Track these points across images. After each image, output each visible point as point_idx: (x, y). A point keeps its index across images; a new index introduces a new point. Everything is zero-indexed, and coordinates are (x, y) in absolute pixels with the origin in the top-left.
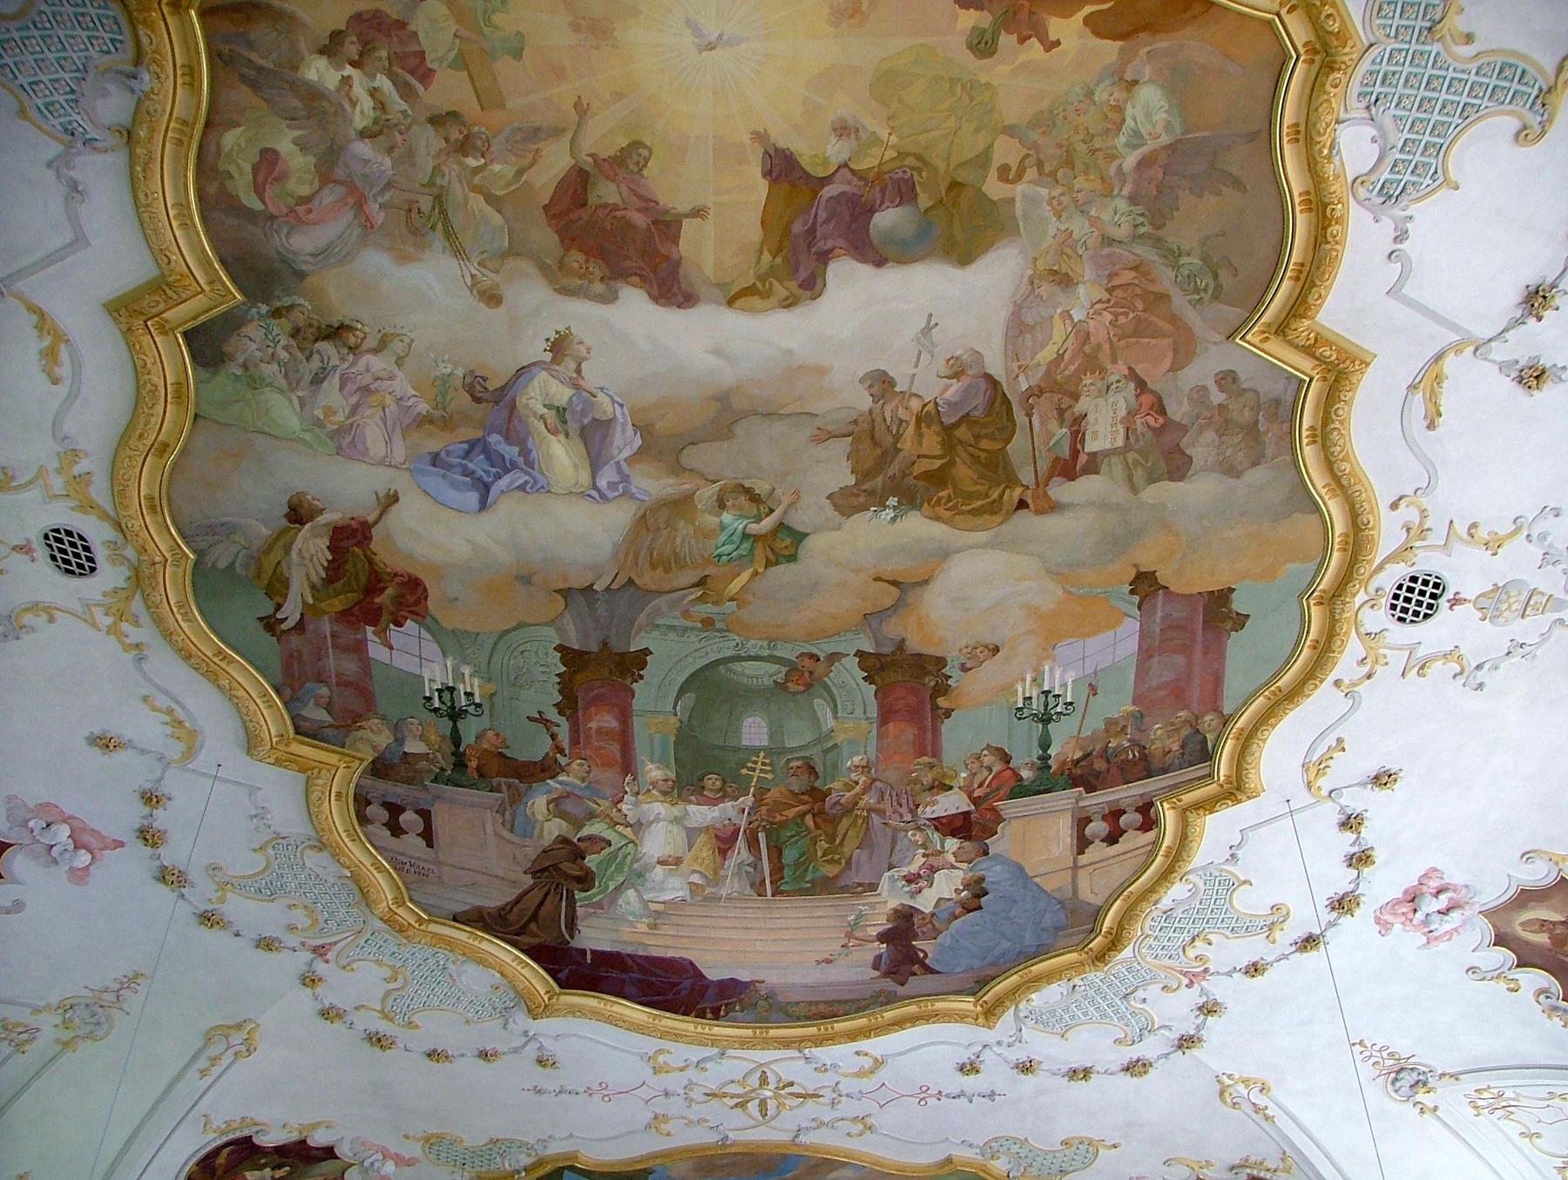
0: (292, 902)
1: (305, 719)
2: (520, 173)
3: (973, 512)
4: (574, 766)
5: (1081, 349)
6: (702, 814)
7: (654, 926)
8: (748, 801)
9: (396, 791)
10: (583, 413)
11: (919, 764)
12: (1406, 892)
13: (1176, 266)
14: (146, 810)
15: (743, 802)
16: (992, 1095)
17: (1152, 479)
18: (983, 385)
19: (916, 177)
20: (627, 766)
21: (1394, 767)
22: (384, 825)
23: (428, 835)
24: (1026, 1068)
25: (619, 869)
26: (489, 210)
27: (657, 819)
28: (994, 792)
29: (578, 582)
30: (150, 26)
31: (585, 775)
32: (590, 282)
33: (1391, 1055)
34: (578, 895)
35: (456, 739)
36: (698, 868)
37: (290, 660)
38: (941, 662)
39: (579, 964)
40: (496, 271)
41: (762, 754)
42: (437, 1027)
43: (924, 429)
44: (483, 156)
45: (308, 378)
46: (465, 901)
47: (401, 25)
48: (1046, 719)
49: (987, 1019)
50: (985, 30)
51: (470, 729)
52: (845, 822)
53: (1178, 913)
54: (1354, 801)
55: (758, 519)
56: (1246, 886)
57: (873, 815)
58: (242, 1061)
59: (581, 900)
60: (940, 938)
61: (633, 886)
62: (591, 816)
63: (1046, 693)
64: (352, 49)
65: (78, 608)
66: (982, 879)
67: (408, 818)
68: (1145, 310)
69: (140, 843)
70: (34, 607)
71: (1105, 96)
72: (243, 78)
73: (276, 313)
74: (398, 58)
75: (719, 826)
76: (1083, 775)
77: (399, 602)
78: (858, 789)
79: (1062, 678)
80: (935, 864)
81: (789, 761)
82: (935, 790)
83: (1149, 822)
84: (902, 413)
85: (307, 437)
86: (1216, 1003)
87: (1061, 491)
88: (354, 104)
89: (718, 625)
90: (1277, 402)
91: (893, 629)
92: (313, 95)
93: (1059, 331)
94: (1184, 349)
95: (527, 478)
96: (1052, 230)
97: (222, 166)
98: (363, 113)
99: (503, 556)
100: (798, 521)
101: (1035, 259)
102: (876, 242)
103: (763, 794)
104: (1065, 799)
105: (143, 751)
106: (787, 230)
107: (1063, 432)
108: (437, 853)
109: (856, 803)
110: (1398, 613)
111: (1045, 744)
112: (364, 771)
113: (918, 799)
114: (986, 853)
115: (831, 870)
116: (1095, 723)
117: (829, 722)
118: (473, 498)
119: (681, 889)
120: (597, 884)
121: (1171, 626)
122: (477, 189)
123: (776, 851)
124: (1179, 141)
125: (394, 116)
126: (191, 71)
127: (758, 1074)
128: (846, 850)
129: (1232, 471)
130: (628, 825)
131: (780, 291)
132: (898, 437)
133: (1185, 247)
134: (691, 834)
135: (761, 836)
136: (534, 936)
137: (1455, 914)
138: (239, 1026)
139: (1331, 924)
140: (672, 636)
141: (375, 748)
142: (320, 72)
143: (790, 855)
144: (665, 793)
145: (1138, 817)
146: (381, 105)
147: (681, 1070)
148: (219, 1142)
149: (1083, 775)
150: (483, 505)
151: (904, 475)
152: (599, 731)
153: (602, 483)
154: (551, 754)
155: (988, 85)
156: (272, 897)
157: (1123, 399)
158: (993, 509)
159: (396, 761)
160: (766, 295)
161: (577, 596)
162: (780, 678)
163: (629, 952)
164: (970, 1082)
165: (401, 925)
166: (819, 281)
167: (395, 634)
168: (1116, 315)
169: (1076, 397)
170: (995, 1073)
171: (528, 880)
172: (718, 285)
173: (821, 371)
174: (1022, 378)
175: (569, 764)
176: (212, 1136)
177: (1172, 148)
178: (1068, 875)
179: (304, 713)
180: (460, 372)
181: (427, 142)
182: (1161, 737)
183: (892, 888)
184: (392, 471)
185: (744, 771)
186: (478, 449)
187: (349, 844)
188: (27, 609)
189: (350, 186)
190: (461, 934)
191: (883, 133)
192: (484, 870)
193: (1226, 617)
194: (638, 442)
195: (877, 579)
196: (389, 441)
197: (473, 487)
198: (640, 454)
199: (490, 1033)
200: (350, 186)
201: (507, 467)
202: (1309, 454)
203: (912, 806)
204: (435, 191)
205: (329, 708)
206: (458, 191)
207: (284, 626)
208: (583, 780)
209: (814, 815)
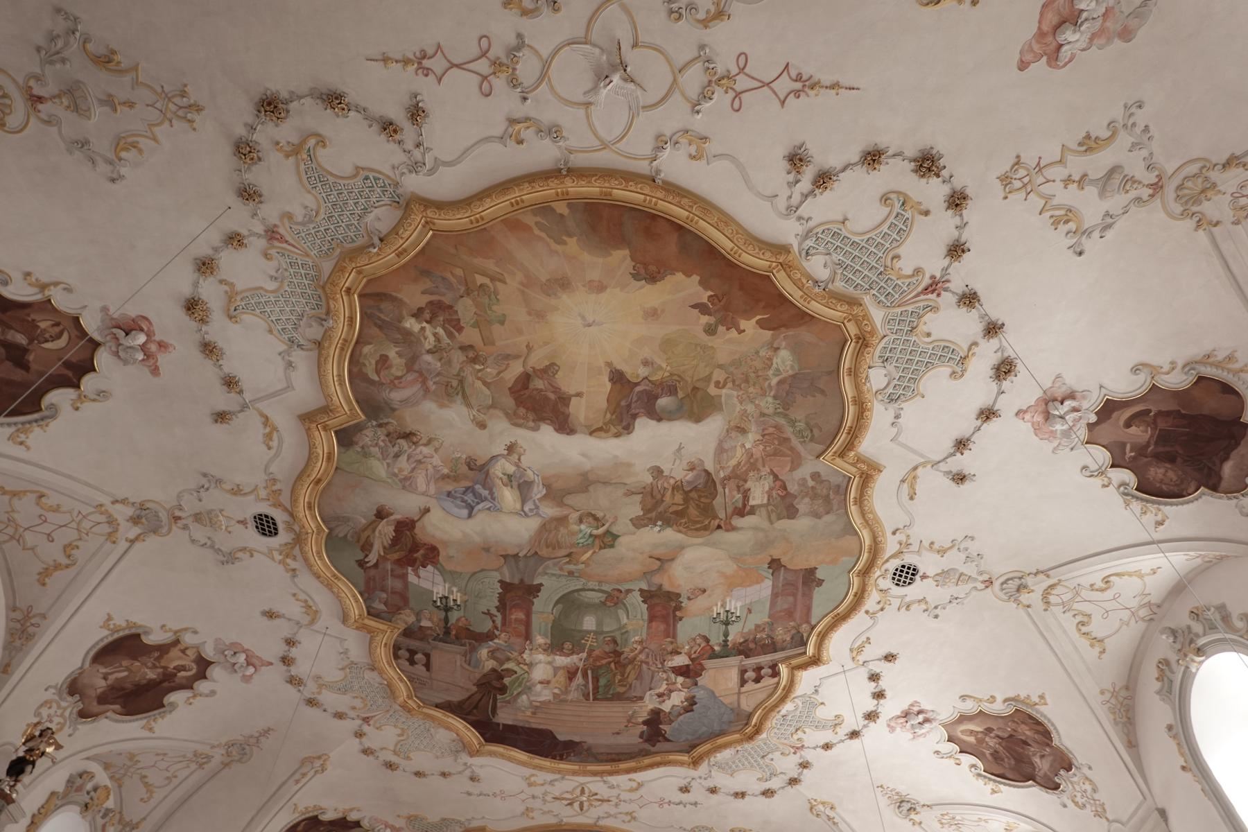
1: (373, 608)
2: (499, 373)
3: (697, 530)
5: (749, 461)
6: (561, 660)
7: (534, 713)
8: (584, 655)
9: (414, 644)
10: (520, 478)
12: (902, 712)
13: (793, 426)
14: (287, 648)
16: (695, 804)
17: (779, 519)
18: (703, 474)
19: (678, 385)
20: (528, 636)
21: (894, 652)
23: (428, 666)
24: (713, 791)
25: (520, 685)
26: (484, 388)
27: (540, 662)
28: (701, 656)
29: (511, 552)
30: (336, 300)
32: (528, 421)
33: (897, 793)
34: (499, 697)
35: (446, 620)
36: (557, 685)
37: (368, 581)
38: (678, 595)
40: (485, 414)
42: (421, 760)
43: (675, 492)
44: (483, 364)
45: (392, 455)
46: (442, 697)
47: (451, 307)
48: (727, 623)
49: (694, 766)
50: (712, 324)
51: (454, 616)
52: (630, 667)
53: (789, 718)
54: (877, 667)
55: (597, 528)
56: (822, 706)
58: (318, 775)
60: (673, 724)
61: (526, 693)
62: (508, 659)
63: (727, 611)
64: (427, 316)
65: (266, 551)
66: (694, 697)
67: (419, 656)
68: (779, 445)
69: (281, 664)
70: (243, 549)
71: (764, 354)
72: (376, 324)
73: (380, 426)
74: (449, 321)
76: (744, 650)
77: (425, 557)
78: (636, 652)
79: (735, 605)
83: (776, 674)
84: (666, 485)
85: (389, 481)
86: (808, 763)
87: (738, 522)
88: (426, 339)
89: (576, 574)
90: (838, 486)
91: (657, 580)
92: (407, 334)
93: (739, 452)
94: (796, 462)
95: (491, 505)
96: (738, 409)
97: (361, 361)
98: (430, 342)
99: (477, 539)
100: (614, 530)
101: (730, 421)
102: (658, 411)
104: (735, 661)
105: (289, 620)
106: (618, 404)
107: (739, 496)
109: (635, 658)
110: (896, 582)
111: (726, 635)
112: (400, 634)
113: (665, 658)
114: (696, 684)
115: (621, 690)
116: (750, 626)
117: (624, 620)
118: (465, 512)
121: (787, 584)
122: (479, 379)
123: (596, 679)
124: (797, 374)
125: (443, 345)
126: (352, 320)
127: (580, 788)
128: (630, 680)
129: (817, 516)
130: (526, 664)
131: (613, 430)
132: (663, 496)
133: (798, 418)
134: (556, 670)
135: (589, 672)
137: (927, 725)
138: (319, 758)
139: (865, 726)
140: (554, 578)
141: (406, 623)
142: (412, 324)
143: (602, 682)
144: (545, 650)
145: (770, 671)
146: (438, 339)
147: (542, 785)
148: (300, 819)
149: (744, 650)
150: (470, 516)
151: (665, 512)
152: (516, 620)
153: (526, 509)
155: (712, 347)
156: (345, 692)
157: (767, 483)
158: (706, 528)
160: (607, 431)
161: (510, 558)
162: (603, 599)
164: (685, 797)
165: (409, 709)
166: (631, 427)
167: (422, 572)
168: (765, 447)
169: (746, 481)
170: (697, 793)
171: (475, 689)
172: (586, 426)
173: (629, 465)
174: (721, 472)
176: (297, 815)
177: (793, 376)
178: (736, 696)
179: (374, 605)
180: (464, 457)
181: (458, 357)
182: (781, 634)
184: (428, 498)
185: (583, 641)
186: (470, 490)
188: (241, 550)
189: (420, 373)
190: (438, 714)
191: (664, 365)
193: (813, 581)
194: (544, 492)
195: (651, 557)
196: (428, 485)
197: (466, 508)
198: (545, 496)
199: (447, 764)
200: (420, 373)
201: (482, 499)
202: (853, 510)
204: (459, 378)
205: (386, 604)
206: (470, 379)
207: (368, 565)
208: (506, 642)
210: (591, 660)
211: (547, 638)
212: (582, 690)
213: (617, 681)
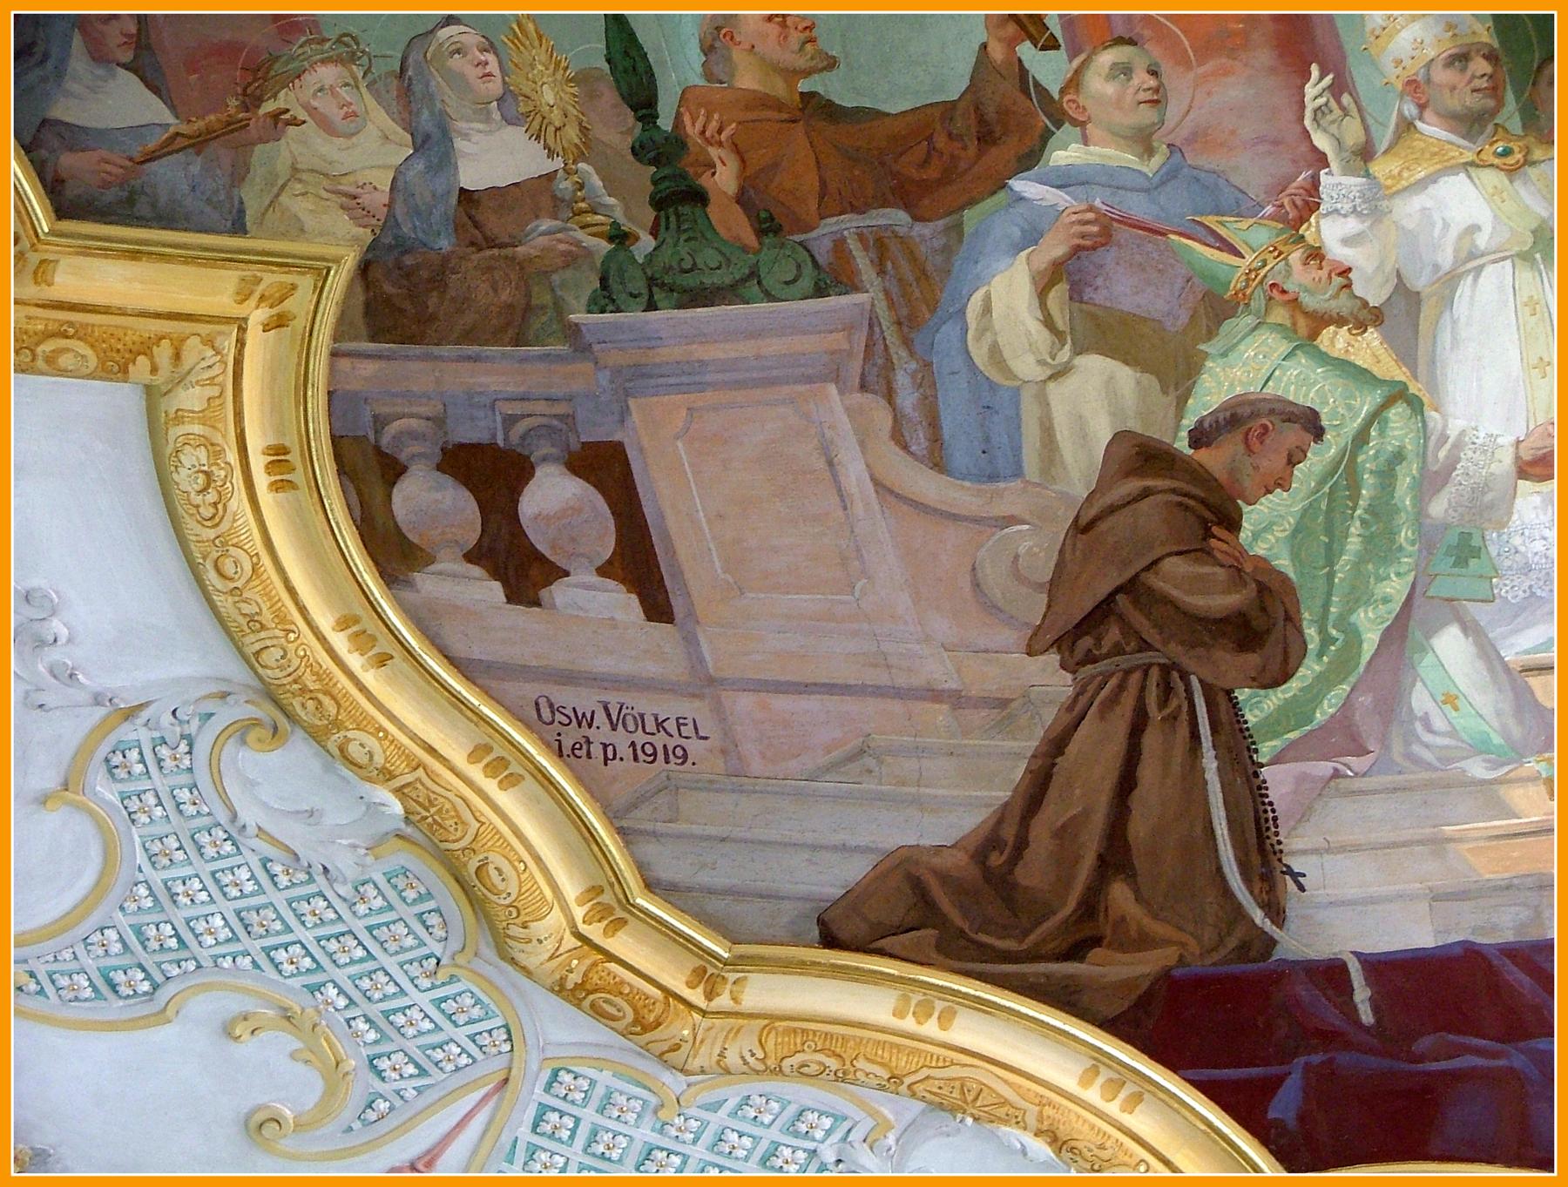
0: (234, 1004)
1: (74, 137)
4: (1098, 84)
22: (470, 557)
25: (1381, 547)
31: (1147, 115)
34: (1258, 706)
39: (1328, 1038)
59: (1275, 725)
61: (1453, 611)
108: (691, 641)
120: (1311, 632)
130: (1367, 317)
136: (1144, 942)
141: (352, 203)
144: (1472, 123)
154: (997, 52)
159: (445, 244)
163: (1508, 936)
175: (1074, 83)
187: (370, 678)
192: (883, 679)
208: (1143, 141)
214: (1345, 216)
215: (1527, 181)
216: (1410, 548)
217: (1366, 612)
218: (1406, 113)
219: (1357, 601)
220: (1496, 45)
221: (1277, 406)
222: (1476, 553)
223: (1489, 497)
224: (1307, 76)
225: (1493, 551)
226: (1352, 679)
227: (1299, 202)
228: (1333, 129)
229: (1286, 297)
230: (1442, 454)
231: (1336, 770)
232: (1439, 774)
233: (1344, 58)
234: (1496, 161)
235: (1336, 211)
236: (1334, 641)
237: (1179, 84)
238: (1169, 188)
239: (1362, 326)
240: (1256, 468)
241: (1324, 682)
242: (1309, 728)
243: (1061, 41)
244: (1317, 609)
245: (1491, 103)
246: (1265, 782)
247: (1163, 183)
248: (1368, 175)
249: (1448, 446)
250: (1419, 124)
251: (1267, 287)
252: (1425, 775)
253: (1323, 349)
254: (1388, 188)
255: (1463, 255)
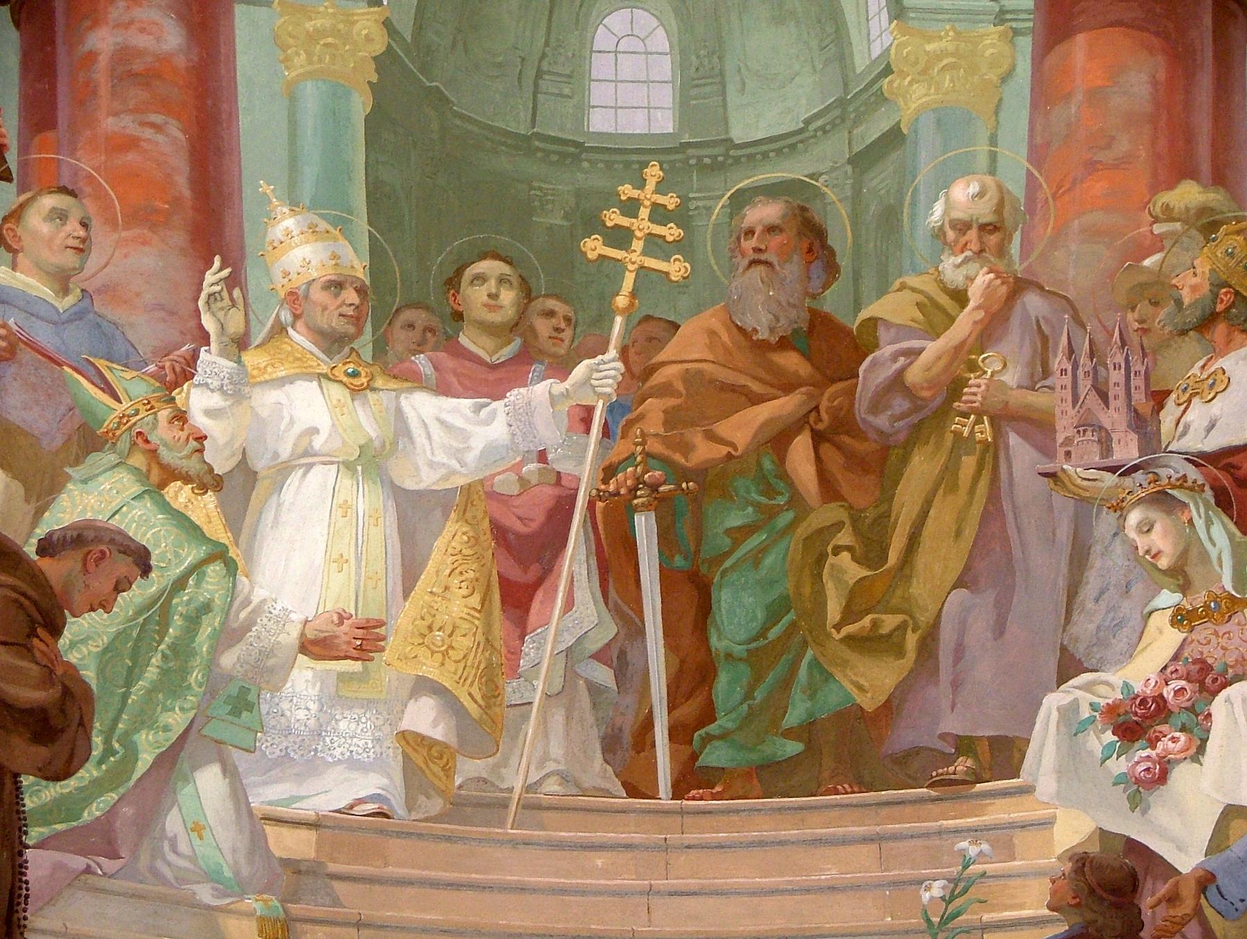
4: (37, 221)
11: (1168, 214)
15: (586, 382)
25: (173, 683)
31: (70, 259)
36: (430, 669)
41: (653, 172)
57: (1013, 439)
59: (48, 813)
61: (219, 752)
75: (507, 484)
80: (1214, 656)
81: (740, 200)
82: (1221, 329)
103: (656, 342)
109: (956, 388)
119: (376, 765)
120: (97, 740)
130: (209, 482)
135: (644, 526)
144: (332, 342)
183: (1072, 754)
185: (594, 246)
203: (1139, 397)
208: (62, 282)
209: (818, 438)
210: (654, 408)
211: (342, 224)
212: (595, 690)
213: (834, 610)
214: (212, 391)
215: (365, 403)
216: (197, 689)
217: (147, 735)
218: (283, 318)
219: (143, 723)
220: (368, 282)
221: (118, 538)
222: (250, 707)
223: (271, 662)
224: (209, 264)
225: (264, 708)
226: (122, 790)
227: (178, 369)
228: (221, 314)
229: (148, 447)
230: (243, 615)
231: (89, 866)
232: (173, 891)
233: (243, 256)
234: (345, 379)
235: (206, 385)
236: (114, 753)
237: (103, 239)
238: (72, 327)
239: (204, 488)
240: (87, 586)
241: (98, 786)
242: (75, 824)
243: (14, 175)
244: (108, 722)
245: (352, 330)
246: (26, 862)
247: (70, 321)
248: (239, 362)
249: (249, 609)
250: (290, 330)
251: (133, 433)
252: (161, 889)
253: (167, 499)
254: (254, 377)
255: (300, 450)
